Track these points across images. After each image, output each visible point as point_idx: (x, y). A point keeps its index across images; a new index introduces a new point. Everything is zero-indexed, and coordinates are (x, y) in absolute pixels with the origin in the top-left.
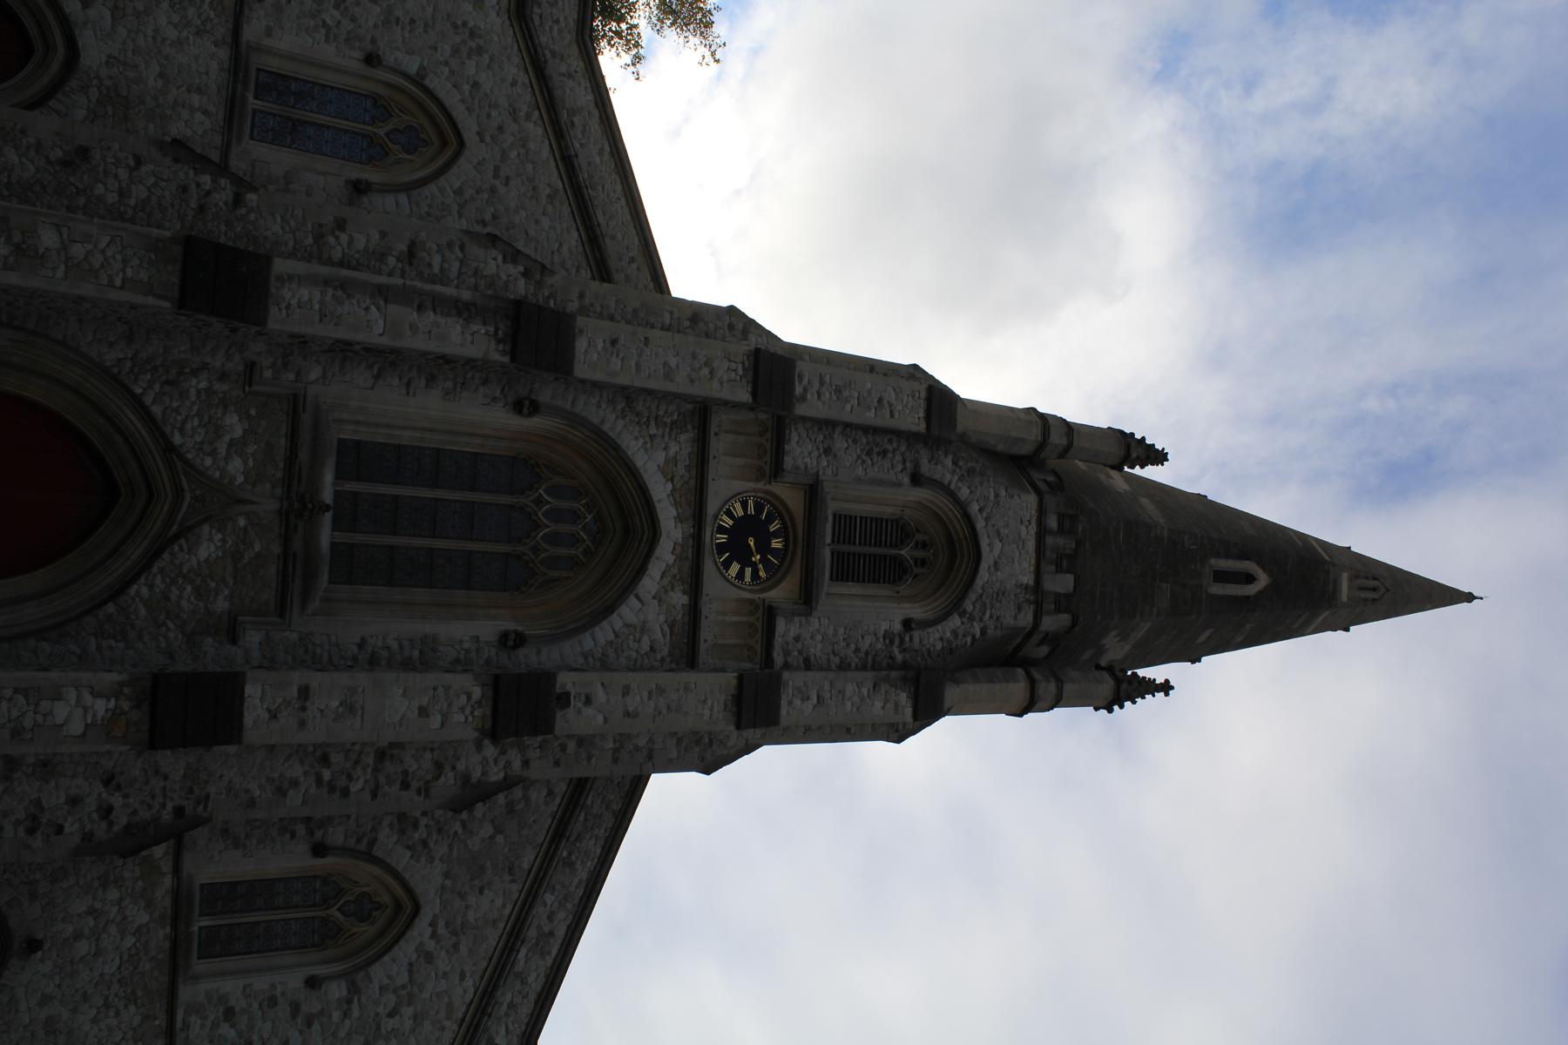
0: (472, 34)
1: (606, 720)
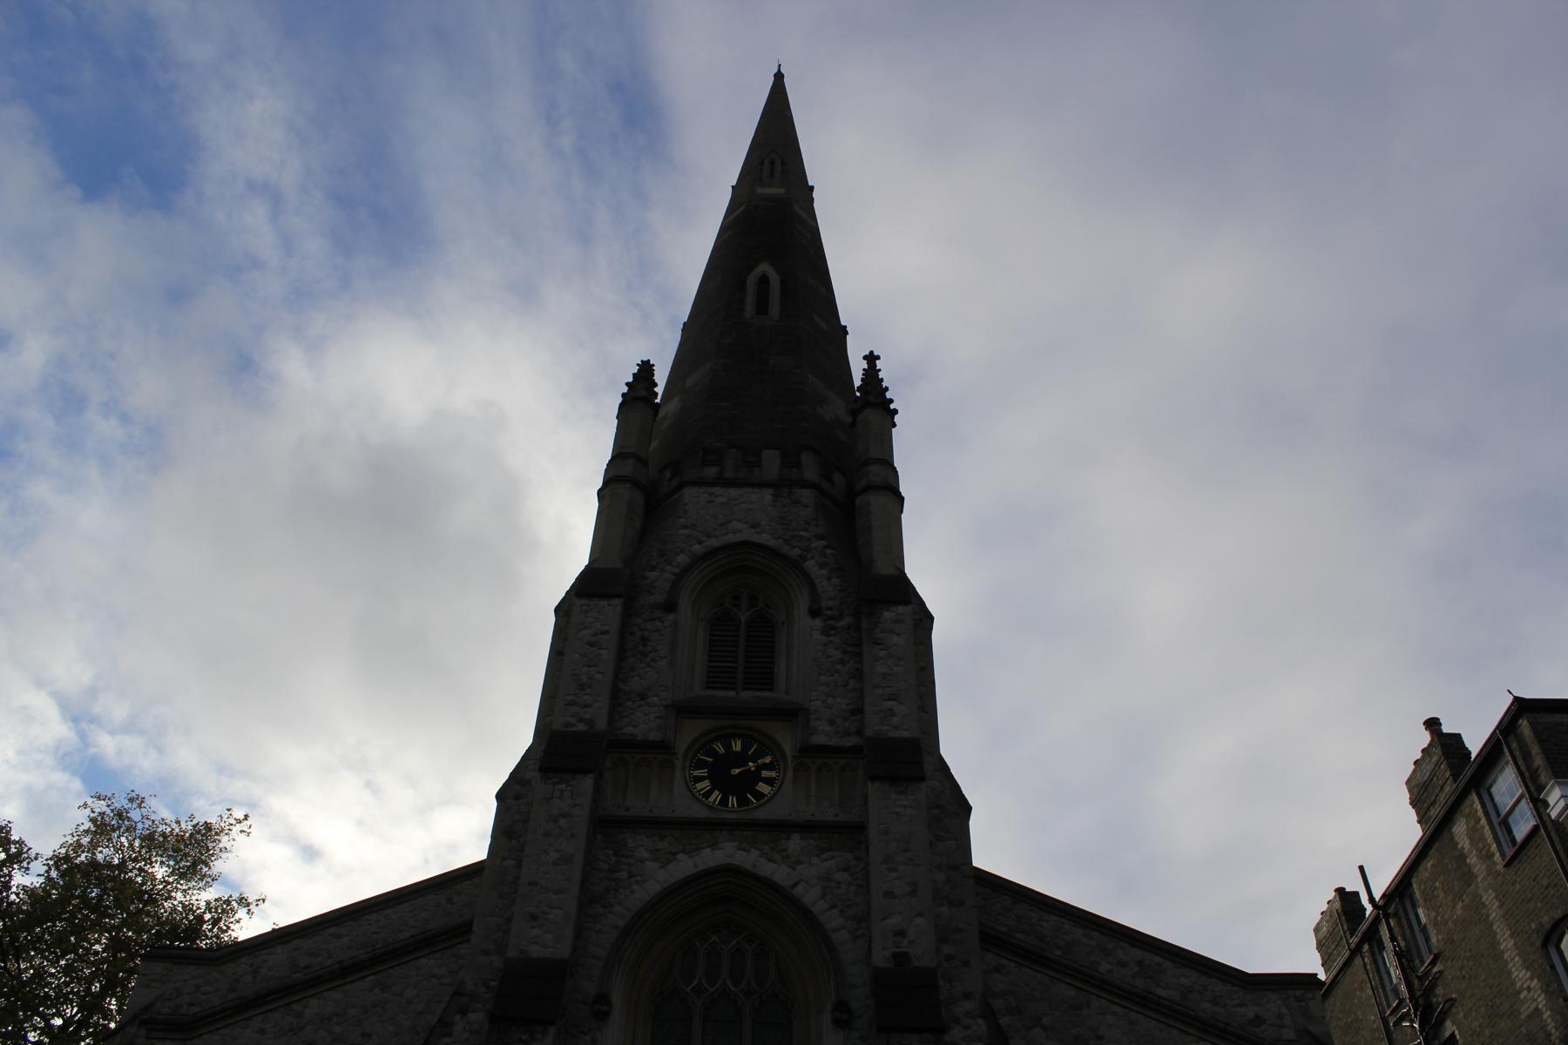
1: (920, 915)
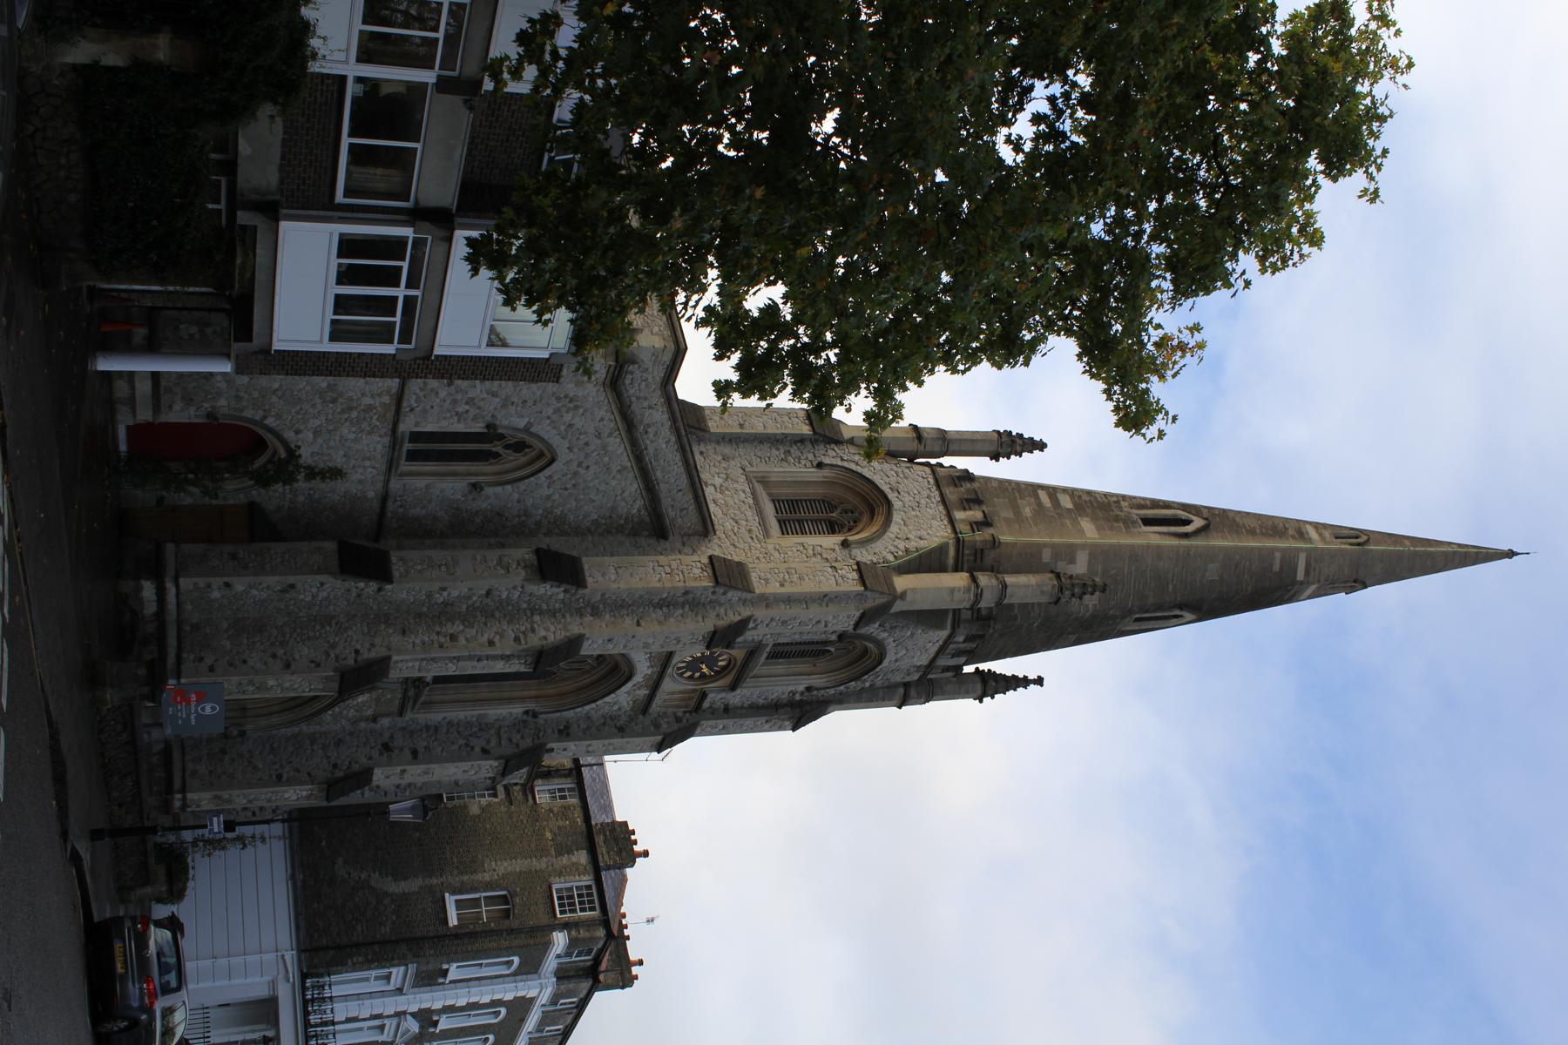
0: (571, 401)
